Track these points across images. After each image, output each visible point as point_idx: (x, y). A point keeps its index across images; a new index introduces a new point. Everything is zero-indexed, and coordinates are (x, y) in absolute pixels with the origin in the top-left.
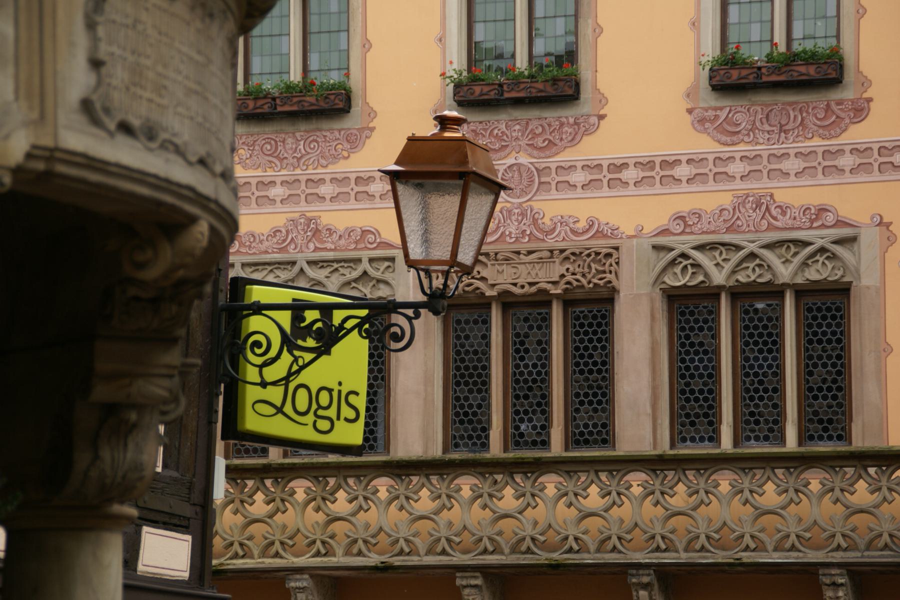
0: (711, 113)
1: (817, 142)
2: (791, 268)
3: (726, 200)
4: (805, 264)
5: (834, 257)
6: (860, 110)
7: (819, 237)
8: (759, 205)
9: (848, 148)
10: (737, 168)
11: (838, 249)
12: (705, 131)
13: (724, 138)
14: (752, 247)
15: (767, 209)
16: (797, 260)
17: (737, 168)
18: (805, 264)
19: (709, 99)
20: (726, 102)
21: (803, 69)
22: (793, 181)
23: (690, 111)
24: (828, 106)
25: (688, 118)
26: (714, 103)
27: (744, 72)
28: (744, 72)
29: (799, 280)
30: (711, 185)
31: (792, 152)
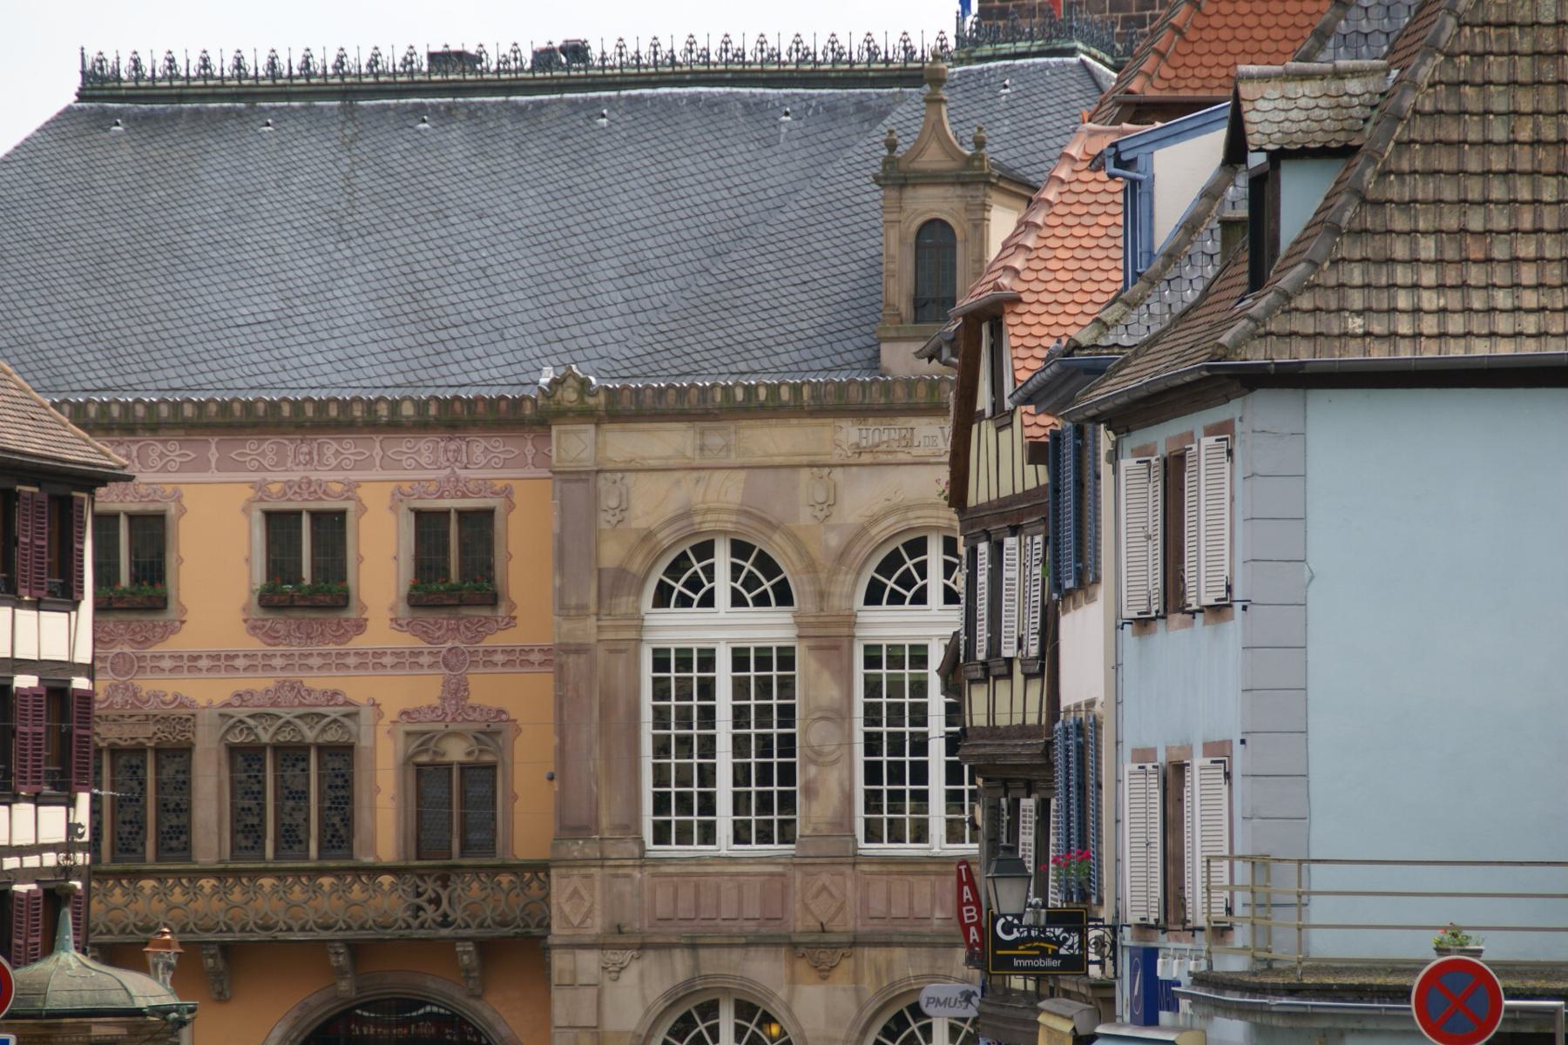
0: (259, 623)
1: (332, 646)
2: (315, 732)
3: (270, 684)
4: (324, 730)
5: (342, 726)
6: (360, 626)
7: (333, 712)
8: (293, 688)
9: (352, 652)
10: (278, 662)
11: (346, 721)
12: (255, 635)
13: (269, 641)
14: (288, 717)
15: (299, 692)
16: (318, 727)
17: (278, 662)
18: (324, 730)
19: (257, 613)
20: (270, 616)
21: (322, 598)
22: (315, 673)
23: (245, 621)
24: (339, 624)
25: (244, 626)
26: (261, 616)
27: (283, 598)
28: (283, 598)
29: (320, 740)
30: (260, 673)
31: (315, 653)
